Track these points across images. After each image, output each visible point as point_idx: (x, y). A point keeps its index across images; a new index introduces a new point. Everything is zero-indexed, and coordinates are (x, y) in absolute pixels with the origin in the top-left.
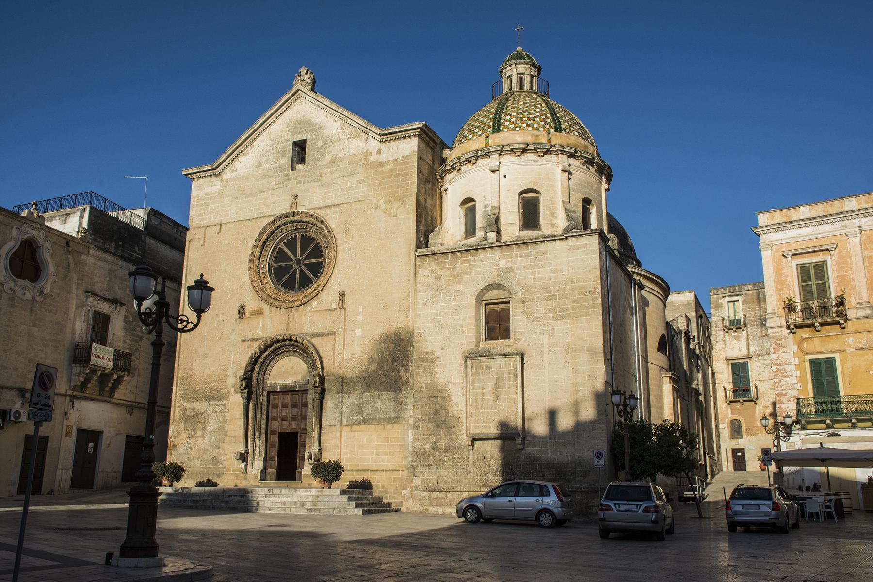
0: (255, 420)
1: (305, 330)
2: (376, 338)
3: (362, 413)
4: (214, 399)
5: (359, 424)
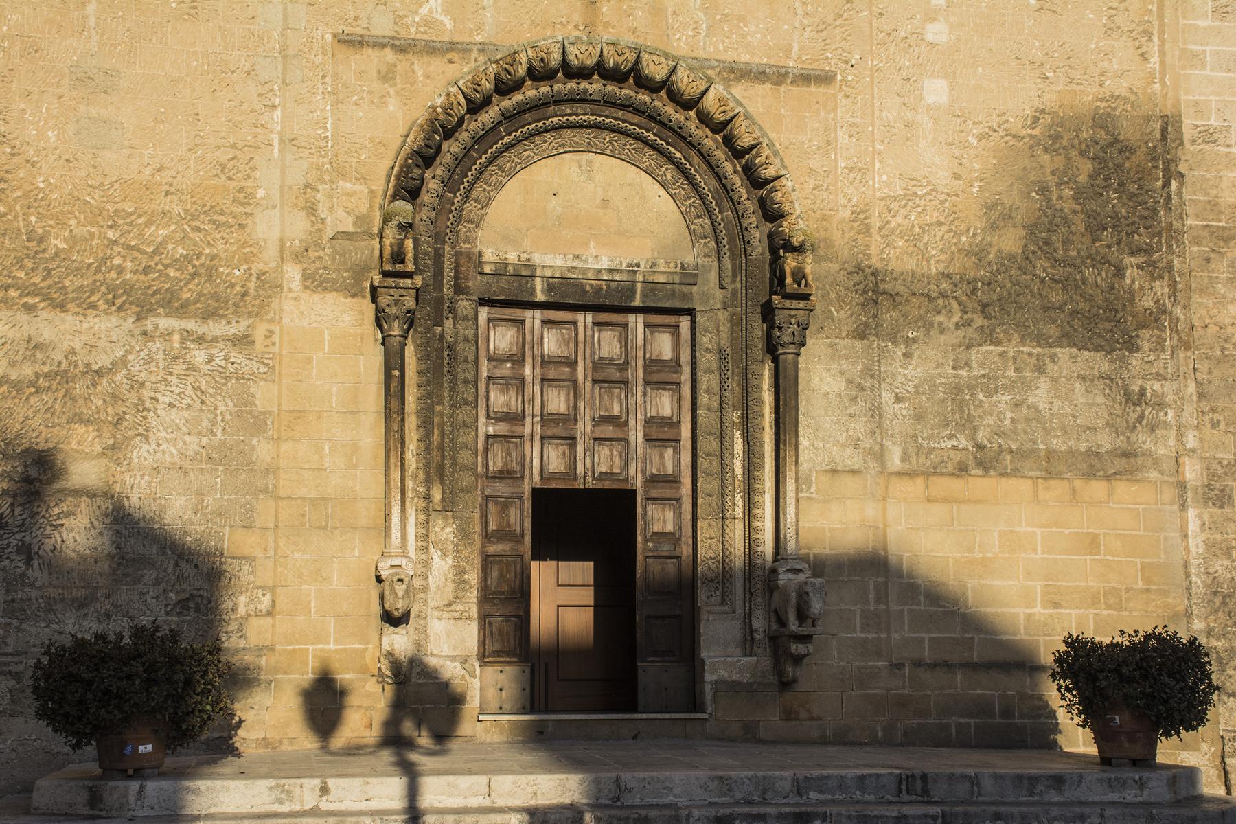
0: (427, 425)
1: (681, 44)
2: (1015, 125)
3: (969, 424)
4: (182, 310)
5: (962, 470)
